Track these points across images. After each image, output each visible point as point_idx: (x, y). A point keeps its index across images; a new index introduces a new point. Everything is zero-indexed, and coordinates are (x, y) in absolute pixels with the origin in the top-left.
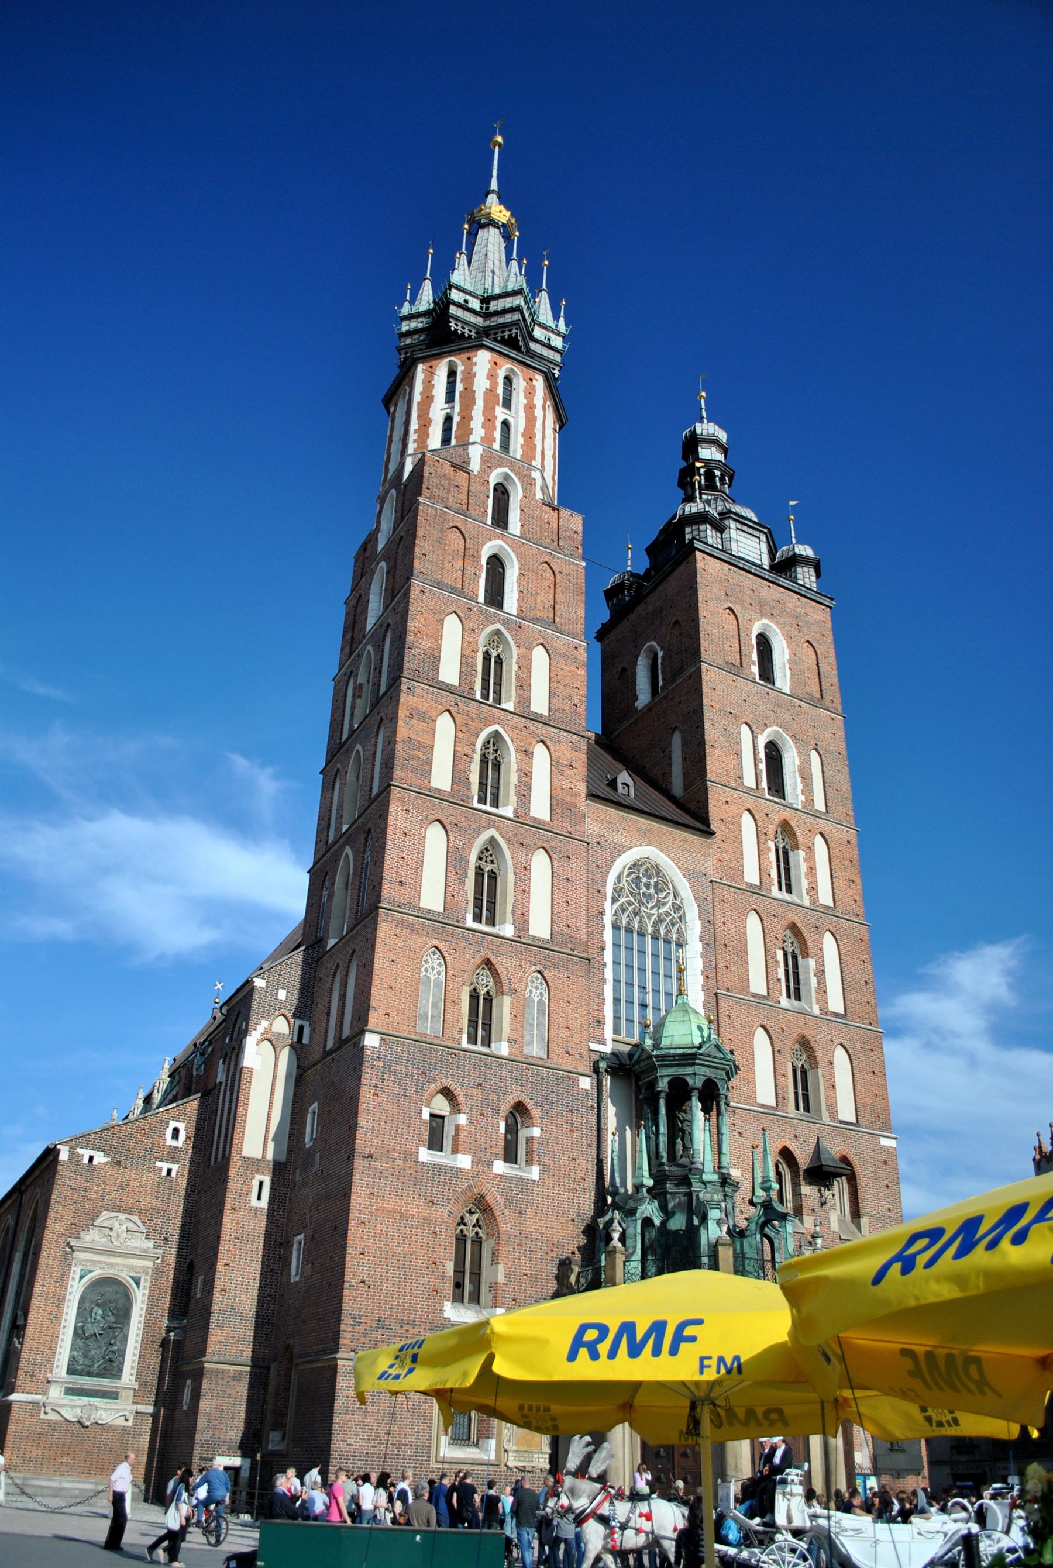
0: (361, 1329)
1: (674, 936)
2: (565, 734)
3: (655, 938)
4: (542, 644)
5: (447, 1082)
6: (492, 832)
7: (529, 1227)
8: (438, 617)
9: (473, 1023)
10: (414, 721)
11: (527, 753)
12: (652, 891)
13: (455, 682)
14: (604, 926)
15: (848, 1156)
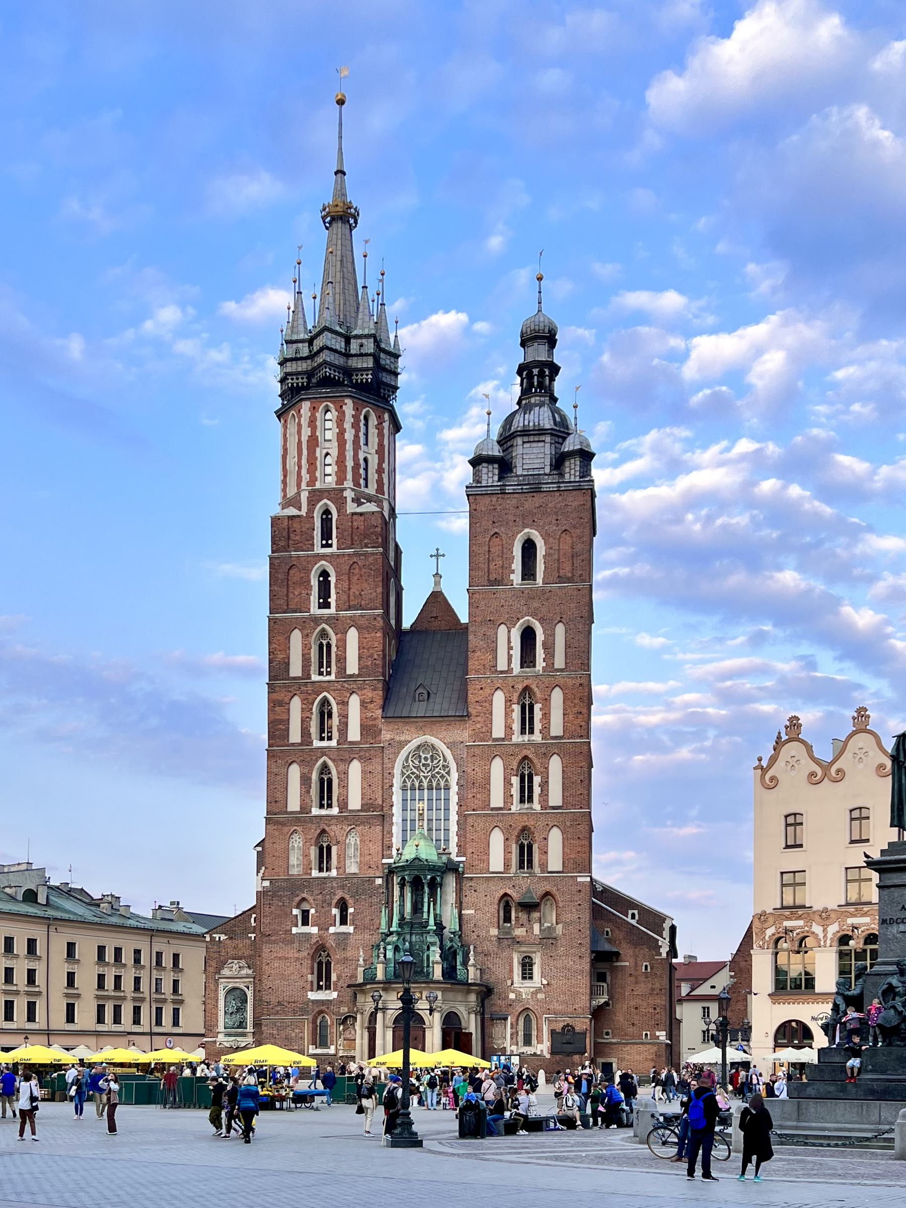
0: (271, 1006)
1: (442, 784)
2: (367, 682)
3: (430, 788)
4: (352, 626)
5: (304, 895)
6: (324, 758)
7: (349, 954)
8: (285, 636)
9: (321, 862)
10: (277, 709)
11: (344, 704)
12: (429, 761)
13: (300, 675)
14: (393, 793)
15: (551, 891)
